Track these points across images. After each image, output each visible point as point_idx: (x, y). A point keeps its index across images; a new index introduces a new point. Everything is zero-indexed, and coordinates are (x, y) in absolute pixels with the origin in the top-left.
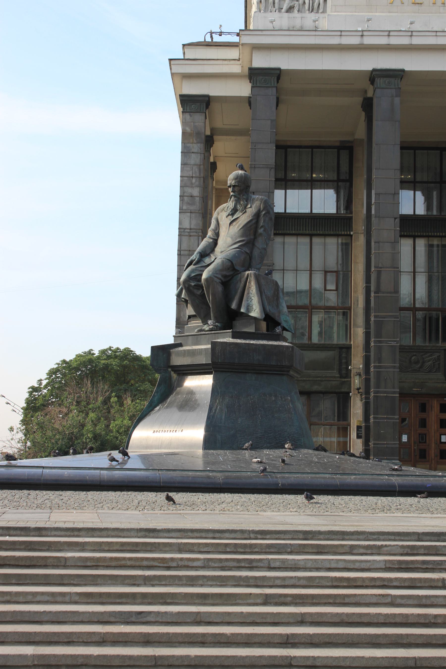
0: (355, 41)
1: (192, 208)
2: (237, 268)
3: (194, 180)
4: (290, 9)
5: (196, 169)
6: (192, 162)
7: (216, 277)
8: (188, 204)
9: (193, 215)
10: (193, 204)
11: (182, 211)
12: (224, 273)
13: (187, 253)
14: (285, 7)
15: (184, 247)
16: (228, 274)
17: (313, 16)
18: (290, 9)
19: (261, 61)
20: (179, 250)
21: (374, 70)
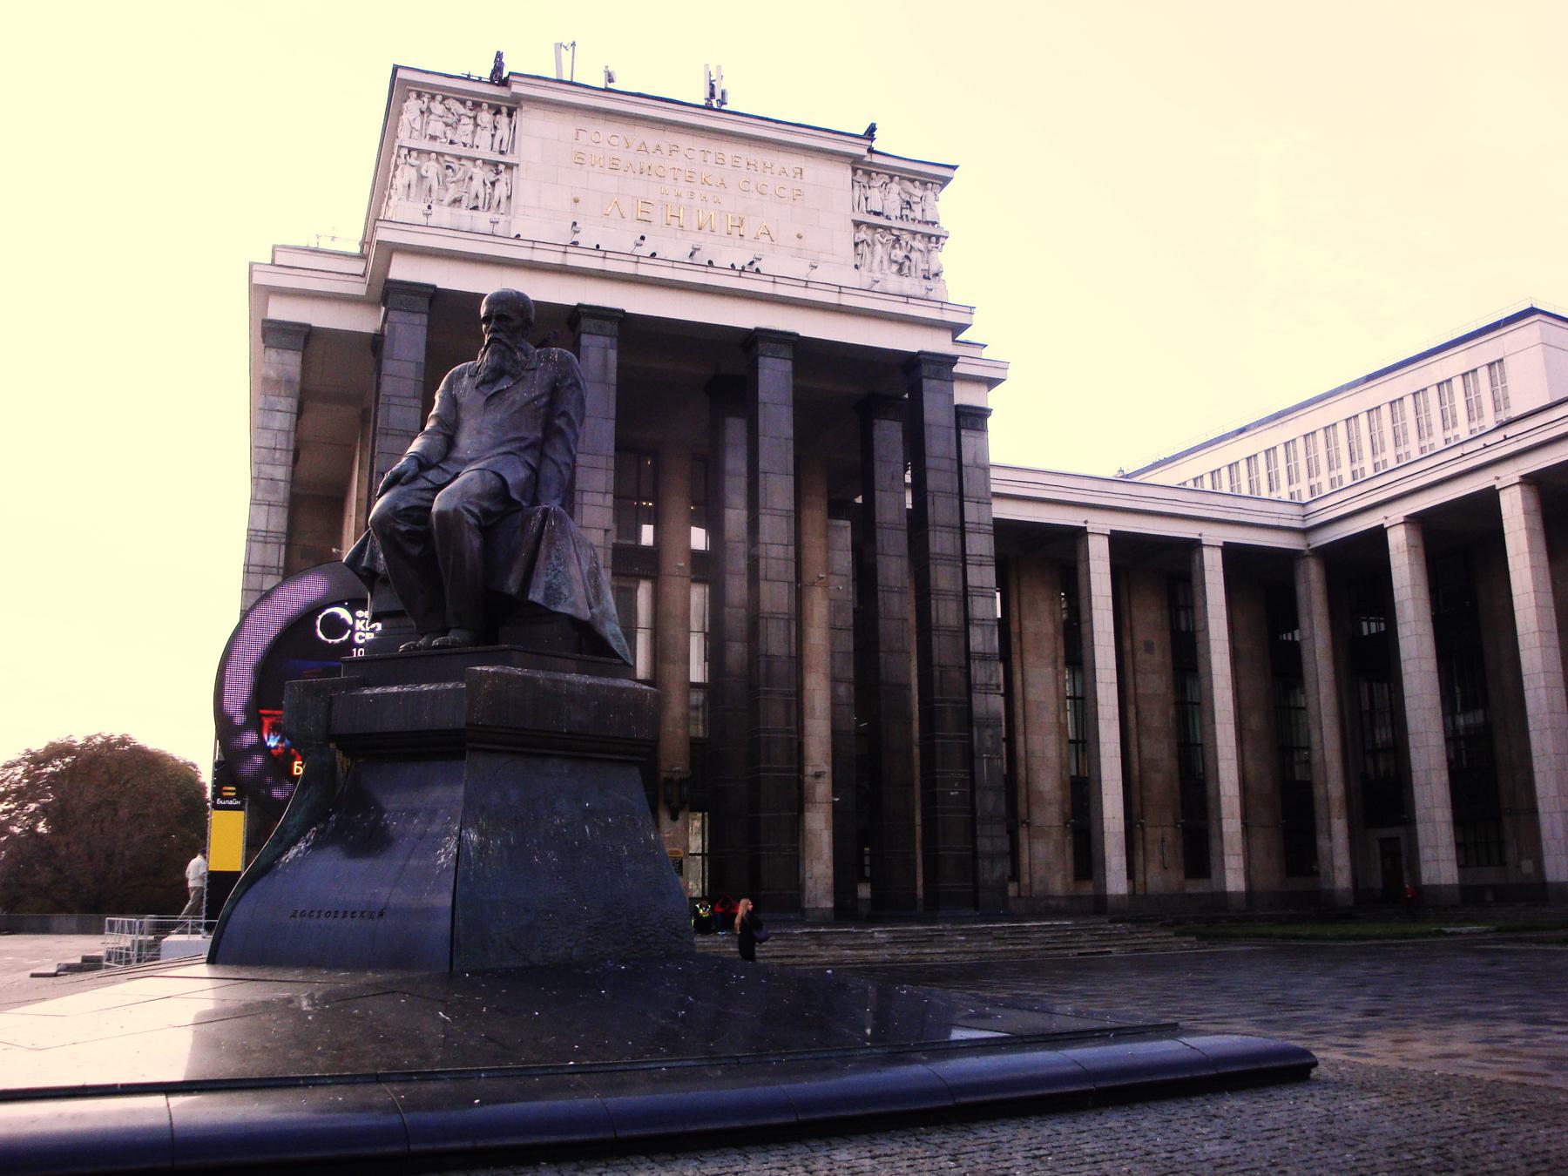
0: (554, 258)
1: (272, 498)
2: (515, 495)
3: (278, 455)
4: (457, 201)
5: (282, 438)
6: (276, 425)
7: (469, 511)
8: (266, 491)
9: (273, 509)
10: (276, 491)
11: (255, 502)
12: (486, 504)
13: (259, 569)
14: (448, 198)
15: (256, 559)
16: (492, 508)
17: (490, 215)
18: (457, 201)
19: (403, 270)
20: (247, 565)
21: (580, 306)
